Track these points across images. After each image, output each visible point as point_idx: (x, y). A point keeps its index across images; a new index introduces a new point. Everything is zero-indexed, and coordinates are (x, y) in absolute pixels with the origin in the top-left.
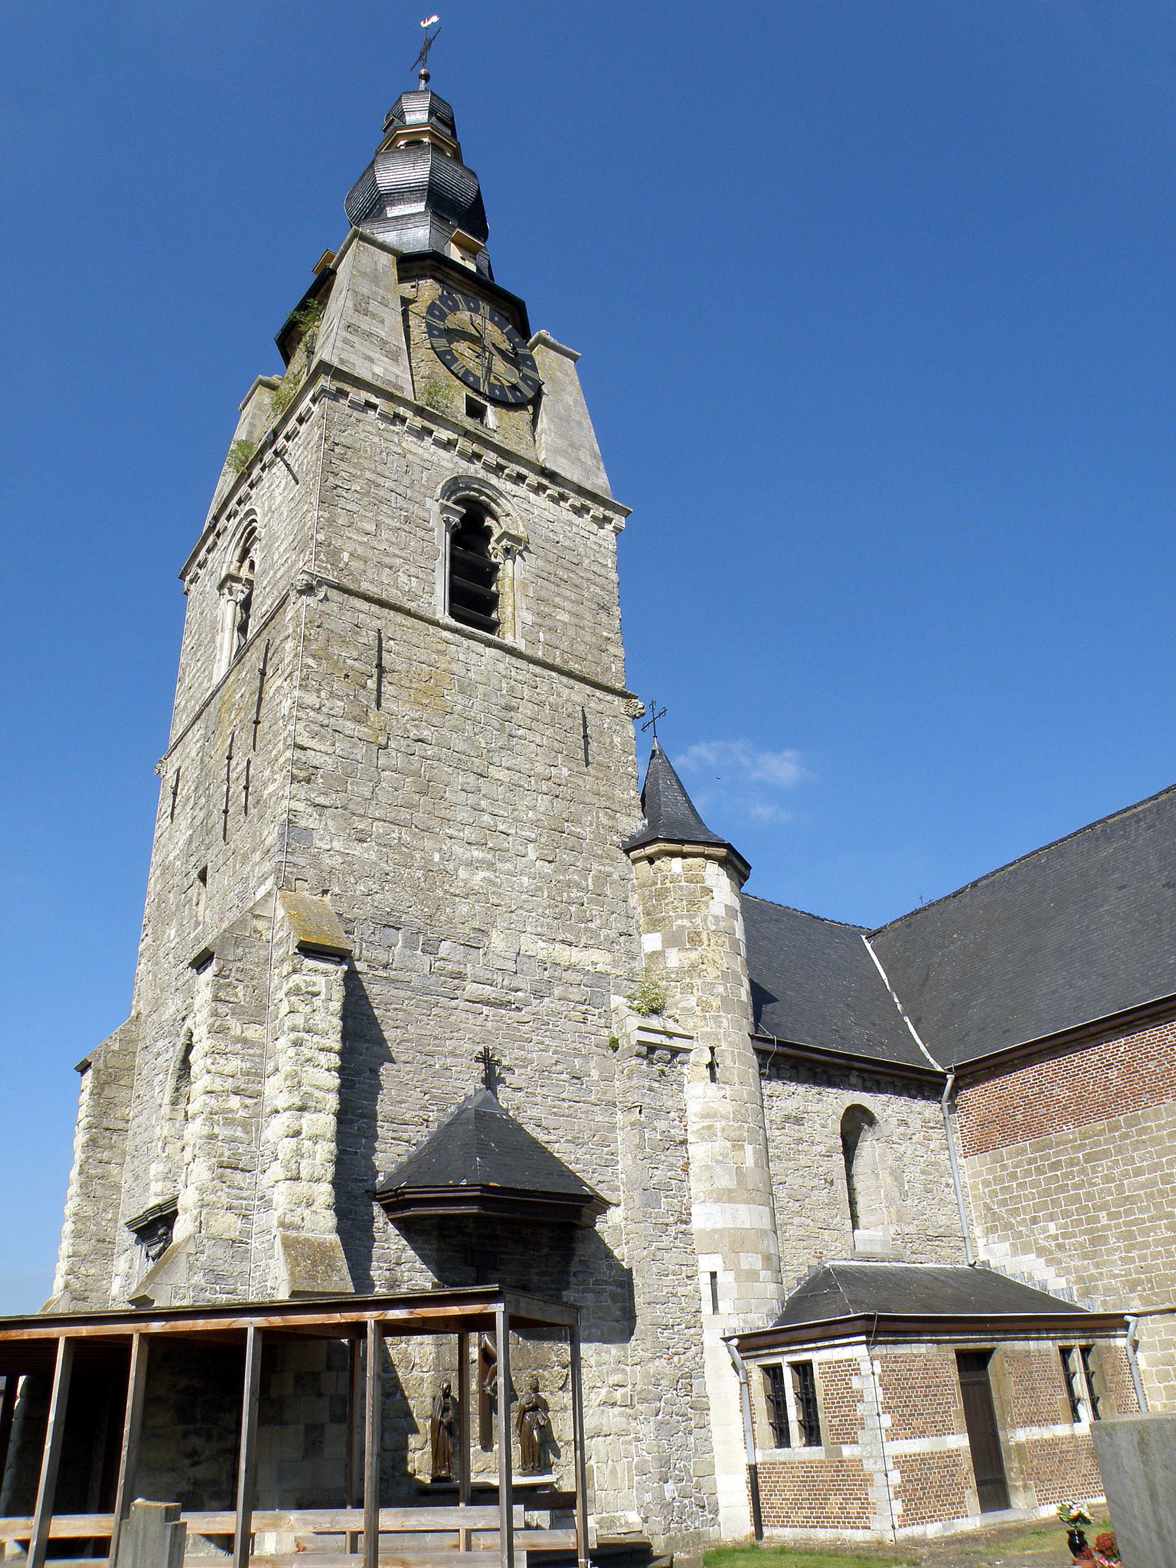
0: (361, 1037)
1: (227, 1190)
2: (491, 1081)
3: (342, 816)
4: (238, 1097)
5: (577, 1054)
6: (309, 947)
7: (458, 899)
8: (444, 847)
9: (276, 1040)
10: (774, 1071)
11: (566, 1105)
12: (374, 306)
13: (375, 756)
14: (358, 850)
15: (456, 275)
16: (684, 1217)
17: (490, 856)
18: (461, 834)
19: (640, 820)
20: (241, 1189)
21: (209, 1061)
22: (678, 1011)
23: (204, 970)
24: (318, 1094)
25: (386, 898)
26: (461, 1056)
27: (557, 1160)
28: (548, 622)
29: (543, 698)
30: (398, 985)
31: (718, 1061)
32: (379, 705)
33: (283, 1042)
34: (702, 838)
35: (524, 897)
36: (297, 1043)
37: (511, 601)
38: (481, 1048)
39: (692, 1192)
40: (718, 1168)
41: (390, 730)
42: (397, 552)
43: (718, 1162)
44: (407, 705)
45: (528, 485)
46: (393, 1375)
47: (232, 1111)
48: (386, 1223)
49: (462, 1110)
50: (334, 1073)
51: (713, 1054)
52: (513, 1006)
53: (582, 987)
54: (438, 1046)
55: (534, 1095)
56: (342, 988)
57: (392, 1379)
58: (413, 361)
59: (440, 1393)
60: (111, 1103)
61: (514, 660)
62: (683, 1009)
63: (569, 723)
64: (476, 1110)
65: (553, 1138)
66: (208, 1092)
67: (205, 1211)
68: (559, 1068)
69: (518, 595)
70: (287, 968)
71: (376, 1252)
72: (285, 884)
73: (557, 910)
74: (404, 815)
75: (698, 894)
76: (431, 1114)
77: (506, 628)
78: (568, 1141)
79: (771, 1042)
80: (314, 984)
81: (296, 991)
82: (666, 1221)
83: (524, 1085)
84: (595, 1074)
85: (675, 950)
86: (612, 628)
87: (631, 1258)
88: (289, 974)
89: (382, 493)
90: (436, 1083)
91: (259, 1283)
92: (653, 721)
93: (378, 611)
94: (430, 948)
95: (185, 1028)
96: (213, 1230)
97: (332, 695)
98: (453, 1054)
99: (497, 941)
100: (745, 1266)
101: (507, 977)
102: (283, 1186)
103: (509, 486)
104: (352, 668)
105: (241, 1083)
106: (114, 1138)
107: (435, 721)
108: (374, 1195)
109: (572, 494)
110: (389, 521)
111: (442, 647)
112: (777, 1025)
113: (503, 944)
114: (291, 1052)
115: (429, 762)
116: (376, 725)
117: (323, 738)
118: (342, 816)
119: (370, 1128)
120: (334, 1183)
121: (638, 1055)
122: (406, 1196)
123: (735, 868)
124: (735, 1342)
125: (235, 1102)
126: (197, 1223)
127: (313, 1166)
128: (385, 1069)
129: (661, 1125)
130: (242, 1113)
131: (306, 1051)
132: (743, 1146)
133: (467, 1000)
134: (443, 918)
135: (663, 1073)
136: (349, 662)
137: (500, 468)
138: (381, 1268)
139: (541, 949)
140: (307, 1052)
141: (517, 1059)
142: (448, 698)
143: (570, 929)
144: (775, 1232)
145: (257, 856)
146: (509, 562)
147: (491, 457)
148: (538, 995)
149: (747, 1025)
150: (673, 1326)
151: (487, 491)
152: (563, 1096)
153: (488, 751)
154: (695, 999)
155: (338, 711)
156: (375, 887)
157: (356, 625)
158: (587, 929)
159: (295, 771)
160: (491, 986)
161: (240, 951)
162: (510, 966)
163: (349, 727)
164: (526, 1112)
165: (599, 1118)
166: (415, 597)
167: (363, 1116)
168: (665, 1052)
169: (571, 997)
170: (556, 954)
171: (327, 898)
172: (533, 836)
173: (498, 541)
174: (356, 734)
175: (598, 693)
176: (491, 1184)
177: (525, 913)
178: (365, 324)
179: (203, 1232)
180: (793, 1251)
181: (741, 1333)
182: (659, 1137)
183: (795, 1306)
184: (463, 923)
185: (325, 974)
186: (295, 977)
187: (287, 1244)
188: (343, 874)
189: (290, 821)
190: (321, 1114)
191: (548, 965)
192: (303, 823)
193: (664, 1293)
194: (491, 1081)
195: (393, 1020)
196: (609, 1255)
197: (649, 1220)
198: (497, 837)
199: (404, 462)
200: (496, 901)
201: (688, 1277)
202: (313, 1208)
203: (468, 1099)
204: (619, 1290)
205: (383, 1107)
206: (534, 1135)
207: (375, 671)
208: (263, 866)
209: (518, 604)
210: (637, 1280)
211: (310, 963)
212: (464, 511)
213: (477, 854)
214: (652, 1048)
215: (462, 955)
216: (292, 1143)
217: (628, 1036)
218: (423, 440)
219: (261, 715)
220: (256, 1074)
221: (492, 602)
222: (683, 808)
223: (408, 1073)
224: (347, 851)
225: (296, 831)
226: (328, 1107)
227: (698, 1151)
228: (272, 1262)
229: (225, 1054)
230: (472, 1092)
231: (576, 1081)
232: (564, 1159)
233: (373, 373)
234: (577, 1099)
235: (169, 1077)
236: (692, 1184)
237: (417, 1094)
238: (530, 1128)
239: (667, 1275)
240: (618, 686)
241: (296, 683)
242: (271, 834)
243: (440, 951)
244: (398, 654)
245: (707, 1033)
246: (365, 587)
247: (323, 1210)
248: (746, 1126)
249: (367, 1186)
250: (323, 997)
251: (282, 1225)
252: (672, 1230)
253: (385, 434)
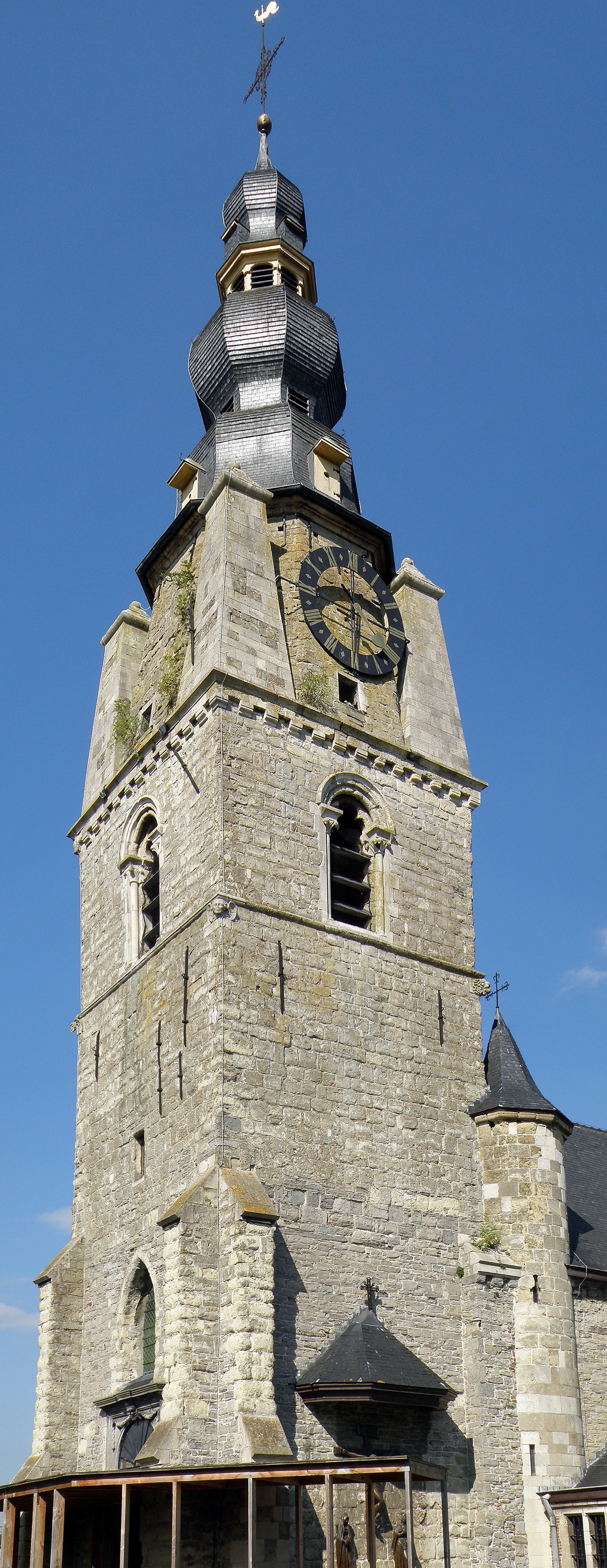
0: (281, 1274)
1: (199, 1385)
2: (372, 1303)
3: (260, 1106)
4: (203, 1321)
5: (433, 1280)
6: (250, 1215)
7: (345, 1165)
8: (335, 1125)
9: (228, 1280)
10: (584, 1291)
11: (425, 1319)
12: (252, 581)
13: (282, 1054)
14: (273, 1132)
16: (511, 1404)
17: (368, 1129)
18: (347, 1113)
19: (484, 1087)
20: (208, 1384)
21: (182, 1296)
22: (510, 1247)
23: (170, 1228)
24: (261, 1320)
25: (294, 1169)
26: (350, 1285)
27: (418, 1360)
29: (407, 986)
30: (306, 1234)
31: (540, 1286)
32: (283, 1009)
33: (234, 1283)
34: (534, 1105)
35: (394, 1159)
36: (245, 1285)
37: (381, 896)
38: (364, 1279)
39: (517, 1385)
40: (538, 1368)
41: (292, 1030)
42: (289, 863)
43: (538, 1363)
44: (304, 1007)
46: (311, 1510)
47: (199, 1331)
48: (303, 1406)
49: (352, 1326)
50: (270, 1304)
51: (536, 1280)
52: (386, 1246)
53: (437, 1228)
54: (334, 1278)
55: (402, 1312)
56: (273, 1243)
57: (309, 1512)
58: (288, 638)
59: (342, 1523)
60: (68, 1309)
62: (514, 1245)
63: (428, 1007)
64: (363, 1326)
65: (415, 1343)
66: (183, 1318)
67: (186, 1400)
68: (420, 1291)
69: (387, 889)
70: (233, 1230)
71: (298, 1426)
72: (223, 1162)
73: (418, 1168)
74: (305, 1101)
75: (529, 1153)
76: (330, 1328)
77: (376, 920)
78: (426, 1346)
79: (583, 1270)
80: (254, 1242)
81: (243, 1247)
82: (498, 1406)
83: (395, 1305)
84: (446, 1295)
85: (509, 1198)
86: (465, 910)
87: (471, 1432)
88: (235, 1234)
90: (334, 1305)
91: (226, 1448)
92: (497, 991)
93: (277, 924)
94: (326, 1205)
95: (134, 1258)
96: (192, 1413)
97: (249, 1005)
98: (345, 1284)
99: (374, 1196)
100: (556, 1441)
101: (382, 1224)
102: (241, 1384)
104: (261, 979)
105: (204, 1311)
106: (72, 1336)
107: (326, 1018)
108: (295, 1386)
110: (280, 832)
111: (327, 950)
112: (590, 1252)
113: (379, 1198)
114: (242, 1291)
115: (322, 1054)
116: (282, 1028)
117: (244, 1043)
118: (260, 1106)
119: (290, 1339)
120: (273, 1381)
121: (479, 1282)
122: (320, 1389)
123: (561, 1128)
124: (547, 1496)
125: (201, 1324)
126: (182, 1408)
127: (260, 1369)
128: (300, 1297)
129: (495, 1334)
130: (205, 1332)
131: (251, 1290)
132: (557, 1351)
133: (354, 1243)
134: (335, 1181)
135: (497, 1295)
136: (259, 974)
138: (300, 1437)
139: (405, 1200)
140: (253, 1292)
141: (389, 1286)
142: (334, 996)
143: (428, 1183)
144: (580, 1417)
145: (197, 1136)
146: (379, 856)
149: (564, 1258)
150: (501, 1482)
152: (423, 1312)
153: (365, 1040)
154: (523, 1237)
155: (253, 1019)
156: (287, 1160)
157: (262, 940)
158: (441, 1182)
159: (225, 1073)
160: (371, 1230)
161: (197, 1216)
162: (384, 1215)
163: (262, 1031)
164: (396, 1325)
165: (448, 1328)
166: (304, 905)
167: (285, 1331)
168: (499, 1279)
169: (429, 1236)
170: (417, 1204)
171: (254, 1171)
173: (370, 834)
174: (268, 1037)
176: (379, 1382)
177: (394, 1173)
178: (246, 606)
179: (186, 1414)
180: (594, 1431)
181: (552, 1490)
182: (493, 1344)
183: (593, 1474)
184: (350, 1184)
185: (261, 1233)
186: (241, 1237)
187: (248, 1423)
188: (264, 1152)
189: (224, 1113)
190: (263, 1334)
191: (412, 1213)
192: (233, 1114)
193: (495, 1459)
194: (372, 1303)
195: (302, 1260)
196: (455, 1429)
197: (485, 1405)
198: (373, 1112)
200: (373, 1165)
201: (513, 1448)
202: (261, 1398)
203: (356, 1316)
204: (462, 1455)
205: (299, 1325)
206: (402, 1342)
207: (278, 979)
208: (203, 1146)
209: (387, 899)
210: (476, 1449)
211: (251, 1227)
212: (341, 812)
214: (489, 1276)
215: (350, 1208)
216: (245, 1355)
217: (471, 1267)
218: (304, 739)
219: (188, 1016)
220: (214, 1305)
221: (362, 896)
222: (520, 1075)
223: (314, 1299)
224: (265, 1133)
225: (229, 1121)
226: (267, 1329)
227: (523, 1355)
228: (235, 1435)
229: (192, 1291)
230: (358, 1311)
231: (432, 1301)
232: (423, 1359)
233: (257, 669)
234: (433, 1314)
235: (122, 1293)
236: (517, 1379)
237: (320, 1314)
238: (399, 1337)
239: (498, 1446)
240: (468, 967)
241: (221, 998)
242: (210, 1123)
243: (334, 1206)
244: (294, 961)
245: (532, 1264)
246: (268, 901)
247: (267, 1400)
248: (560, 1336)
249: (290, 1380)
250: (260, 1250)
251: (242, 1410)
252: (502, 1413)
253: (273, 740)
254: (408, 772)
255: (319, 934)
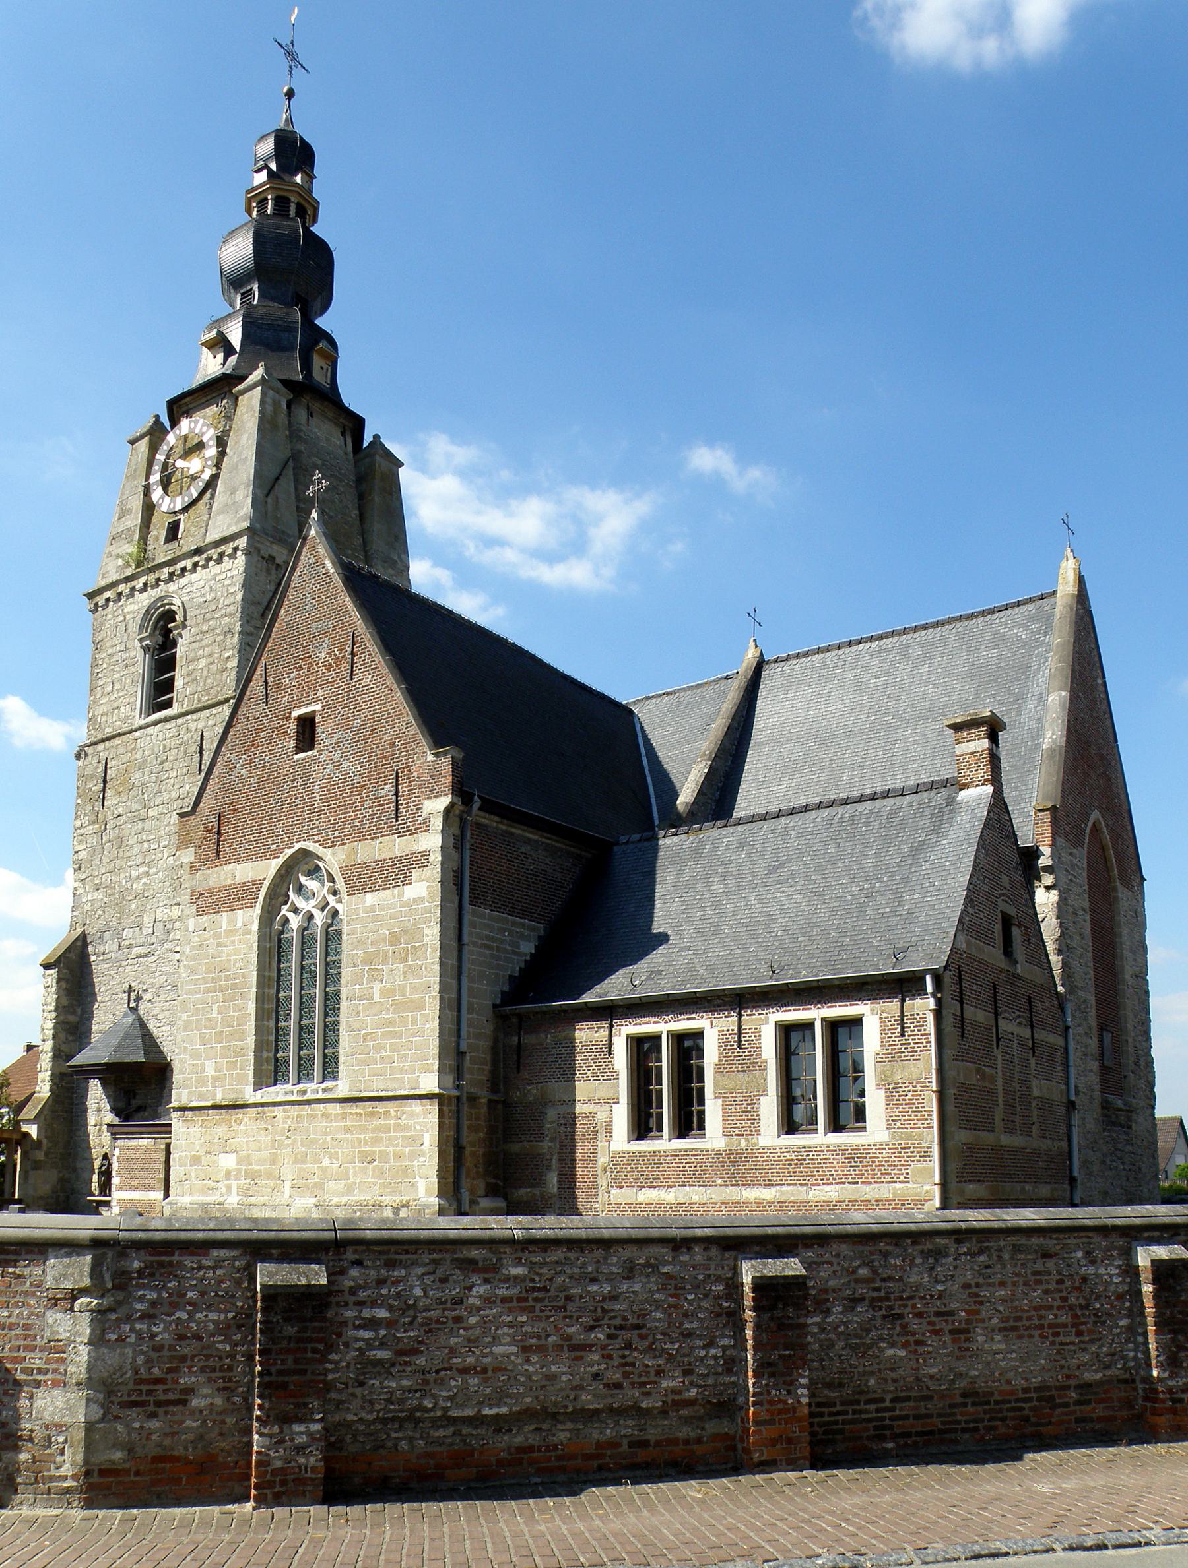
15: (188, 399)
28: (193, 676)
45: (190, 571)
61: (168, 725)
89: (116, 658)
99: (146, 919)
103: (183, 581)
109: (213, 551)
137: (171, 574)
147: (164, 573)
148: (162, 943)
151: (165, 602)
163: (91, 829)
172: (166, 843)
175: (214, 711)
199: (124, 624)
213: (142, 870)
254: (196, 565)
255: (130, 736)
